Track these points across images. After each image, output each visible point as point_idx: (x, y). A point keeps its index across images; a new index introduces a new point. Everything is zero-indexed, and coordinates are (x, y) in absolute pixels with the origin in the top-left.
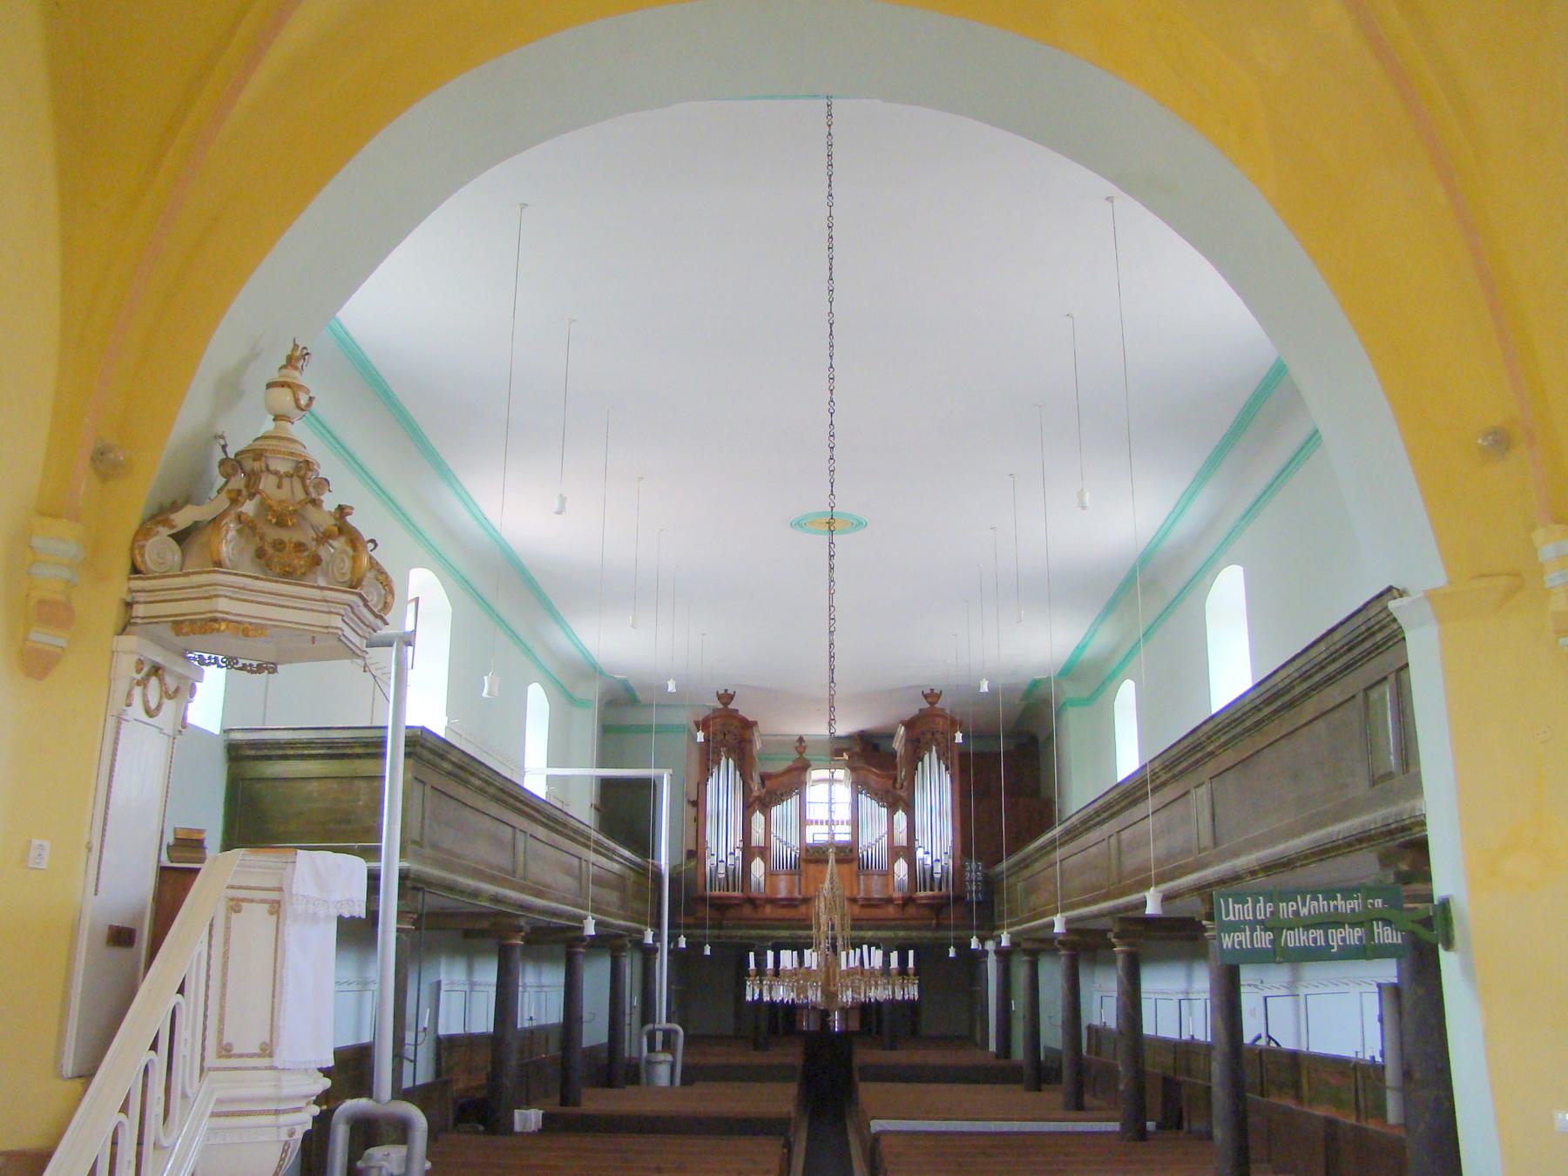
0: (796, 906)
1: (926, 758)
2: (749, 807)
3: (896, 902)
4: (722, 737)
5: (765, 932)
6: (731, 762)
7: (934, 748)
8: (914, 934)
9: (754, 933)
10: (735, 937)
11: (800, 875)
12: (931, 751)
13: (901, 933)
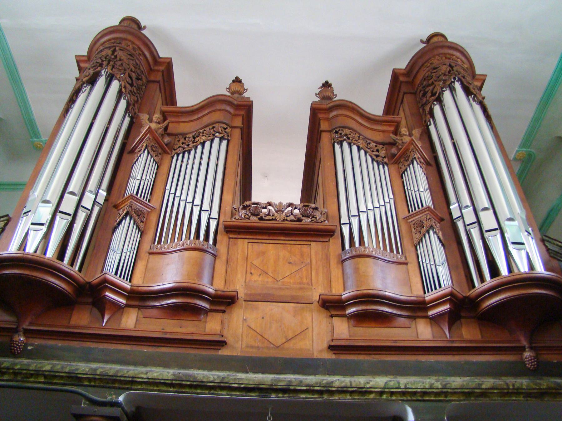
0: (196, 311)
1: (447, 95)
2: (132, 151)
3: (431, 313)
4: (109, 52)
5: (112, 369)
6: (115, 85)
7: (457, 85)
8: (488, 382)
9: (83, 367)
10: (37, 373)
11: (215, 256)
12: (453, 90)
13: (456, 382)
